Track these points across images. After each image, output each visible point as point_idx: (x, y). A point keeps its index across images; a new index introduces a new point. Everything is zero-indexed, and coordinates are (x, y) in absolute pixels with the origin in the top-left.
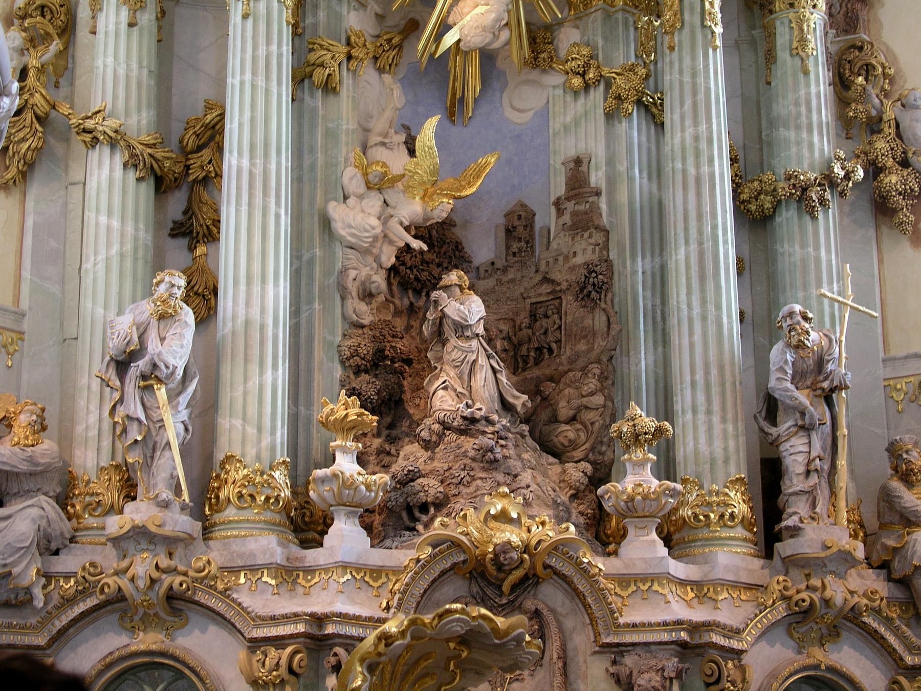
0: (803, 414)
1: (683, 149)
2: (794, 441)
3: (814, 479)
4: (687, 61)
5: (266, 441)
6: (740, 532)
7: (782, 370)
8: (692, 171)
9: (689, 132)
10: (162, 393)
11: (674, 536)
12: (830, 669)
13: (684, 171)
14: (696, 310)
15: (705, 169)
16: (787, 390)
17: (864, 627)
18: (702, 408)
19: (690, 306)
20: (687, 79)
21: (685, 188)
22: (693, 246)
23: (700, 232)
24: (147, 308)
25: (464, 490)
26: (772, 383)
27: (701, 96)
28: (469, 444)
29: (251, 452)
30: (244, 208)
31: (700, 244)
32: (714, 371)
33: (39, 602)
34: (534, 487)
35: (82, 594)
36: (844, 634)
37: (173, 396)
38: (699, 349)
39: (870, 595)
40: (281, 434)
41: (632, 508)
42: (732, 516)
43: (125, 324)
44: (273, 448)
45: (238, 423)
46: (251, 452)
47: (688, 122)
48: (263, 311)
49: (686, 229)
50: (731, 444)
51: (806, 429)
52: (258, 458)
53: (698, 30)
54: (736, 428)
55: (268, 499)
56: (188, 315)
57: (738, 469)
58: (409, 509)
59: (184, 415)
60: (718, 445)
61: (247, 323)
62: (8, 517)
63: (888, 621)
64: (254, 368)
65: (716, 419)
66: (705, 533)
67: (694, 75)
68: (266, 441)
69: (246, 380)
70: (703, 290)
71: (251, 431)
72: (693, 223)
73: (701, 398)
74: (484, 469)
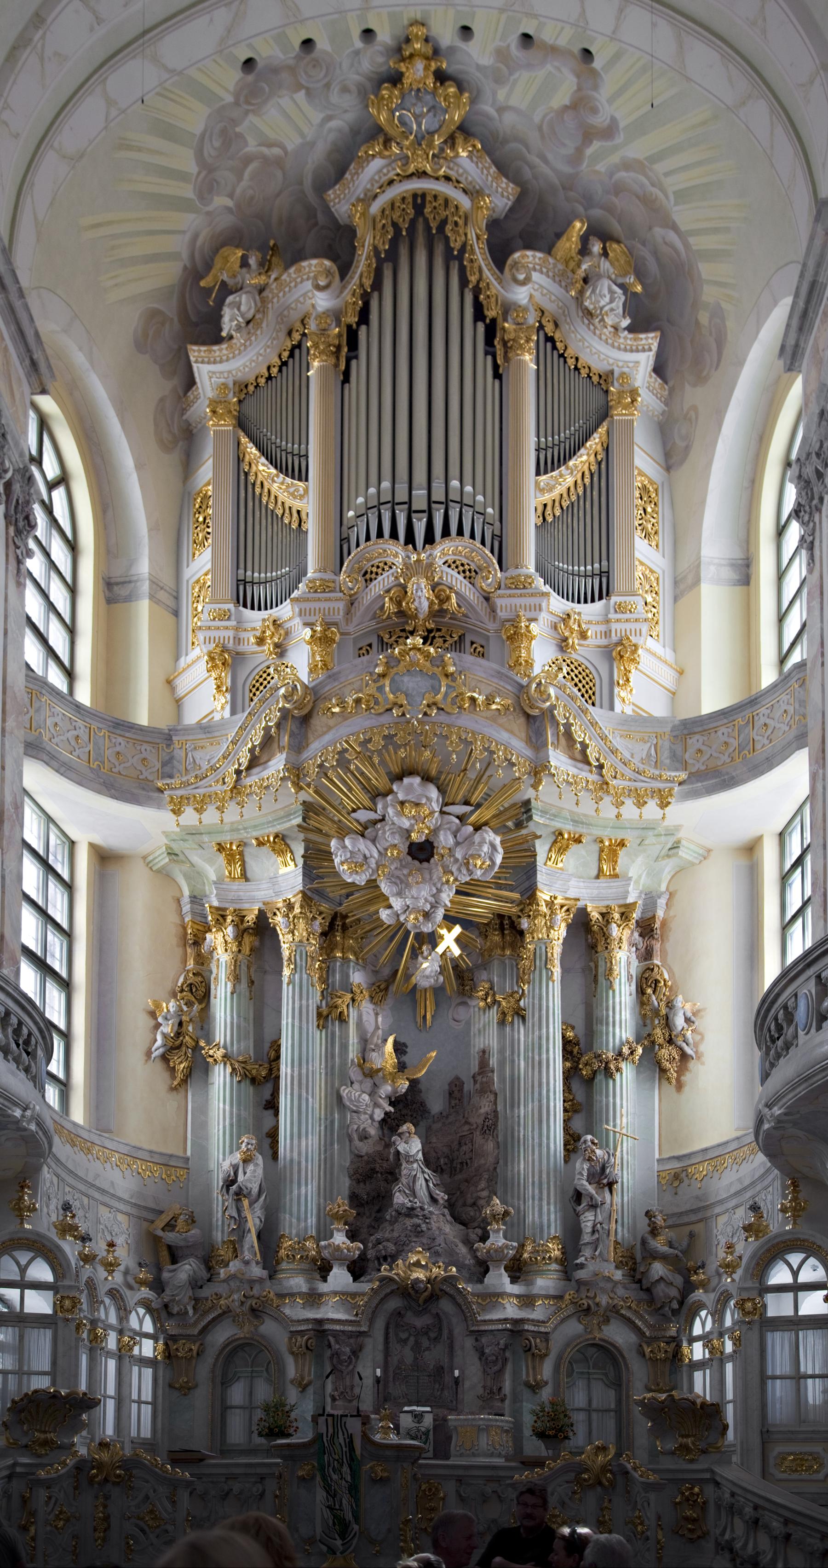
0: (591, 1198)
1: (533, 1044)
2: (587, 1214)
3: (596, 1236)
4: (537, 991)
5: (303, 1224)
6: (554, 1266)
7: (581, 1174)
8: (537, 1058)
9: (537, 1033)
10: (246, 1203)
11: (518, 1270)
12: (600, 1339)
13: (533, 1058)
14: (536, 1141)
15: (544, 1056)
16: (582, 1185)
17: (622, 1316)
18: (537, 1197)
19: (533, 1138)
20: (536, 1002)
21: (533, 1068)
22: (536, 1103)
23: (540, 1094)
24: (237, 1157)
25: (406, 1248)
26: (576, 1181)
27: (544, 1012)
28: (409, 1222)
29: (294, 1232)
30: (289, 1096)
31: (540, 1101)
32: (544, 1176)
33: (191, 1312)
34: (443, 1245)
35: (213, 1307)
36: (612, 1321)
37: (251, 1204)
38: (537, 1163)
39: (625, 1300)
40: (312, 1221)
41: (496, 1256)
42: (550, 1258)
43: (226, 1165)
44: (306, 1228)
45: (287, 1216)
46: (294, 1232)
47: (536, 1028)
48: (299, 1154)
49: (533, 1093)
50: (552, 1217)
51: (593, 1206)
52: (298, 1235)
53: (544, 972)
54: (555, 1207)
55: (302, 1257)
56: (260, 1160)
57: (555, 1229)
58: (378, 1259)
59: (259, 1213)
60: (545, 1218)
61: (292, 1160)
62: (174, 1270)
63: (636, 1312)
64: (295, 1186)
65: (545, 1203)
66: (535, 1268)
67: (540, 999)
68: (303, 1224)
69: (291, 1192)
70: (540, 1128)
71: (294, 1221)
72: (536, 1089)
73: (537, 1191)
74: (417, 1236)
